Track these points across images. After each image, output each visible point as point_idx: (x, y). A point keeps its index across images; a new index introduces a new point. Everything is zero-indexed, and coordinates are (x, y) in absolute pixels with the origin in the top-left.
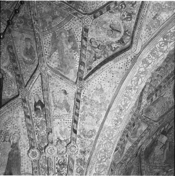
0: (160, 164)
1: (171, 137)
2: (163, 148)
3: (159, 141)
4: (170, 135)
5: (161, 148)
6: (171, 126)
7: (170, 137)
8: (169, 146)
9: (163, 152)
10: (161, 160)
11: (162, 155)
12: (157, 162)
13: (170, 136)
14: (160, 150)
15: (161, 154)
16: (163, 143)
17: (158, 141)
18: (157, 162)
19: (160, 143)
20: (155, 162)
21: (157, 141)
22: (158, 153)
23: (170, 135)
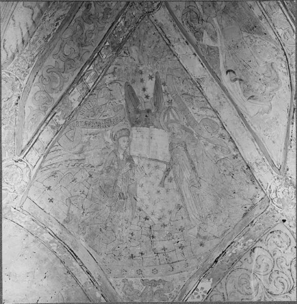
0: (181, 247)
1: (176, 121)
2: (170, 180)
3: (140, 157)
4: (171, 117)
5: (162, 184)
6: (151, 78)
7: (176, 125)
8: (188, 164)
9: (178, 197)
10: (181, 230)
11: (179, 207)
12: (167, 244)
13: (172, 122)
14: (162, 190)
15: (172, 207)
16: (160, 158)
17: (136, 160)
18: (167, 244)
19: (153, 164)
20: (159, 246)
21: (130, 159)
22: (159, 206)
23: (171, 117)
